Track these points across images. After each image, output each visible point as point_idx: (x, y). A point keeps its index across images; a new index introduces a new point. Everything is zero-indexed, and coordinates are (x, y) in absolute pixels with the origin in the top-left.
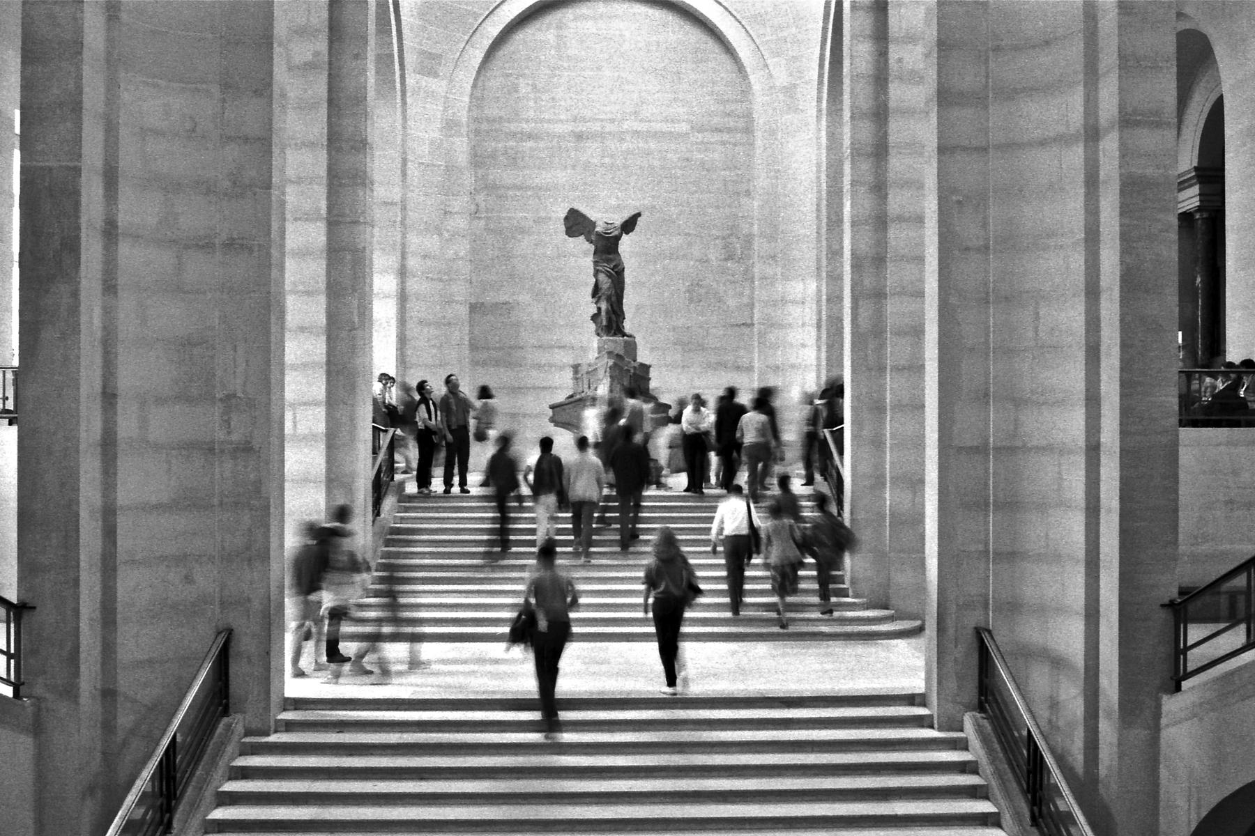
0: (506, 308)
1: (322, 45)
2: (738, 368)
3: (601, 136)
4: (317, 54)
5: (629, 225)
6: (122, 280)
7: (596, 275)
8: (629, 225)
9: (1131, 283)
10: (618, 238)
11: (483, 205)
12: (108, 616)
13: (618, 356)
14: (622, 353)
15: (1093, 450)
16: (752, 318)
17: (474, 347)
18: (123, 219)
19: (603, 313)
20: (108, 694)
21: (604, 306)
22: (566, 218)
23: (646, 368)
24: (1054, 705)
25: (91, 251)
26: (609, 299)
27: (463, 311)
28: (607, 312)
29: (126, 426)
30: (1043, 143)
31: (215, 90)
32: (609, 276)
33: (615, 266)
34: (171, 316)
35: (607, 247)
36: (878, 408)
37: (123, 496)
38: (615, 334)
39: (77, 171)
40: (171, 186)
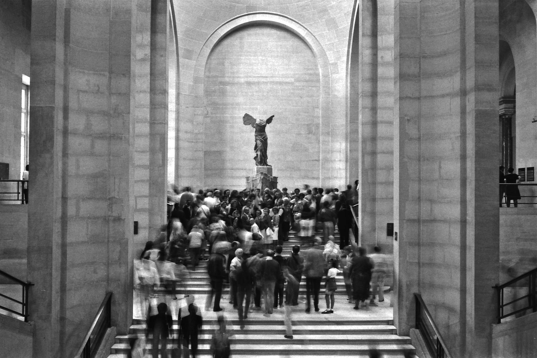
1: (148, 51)
3: (258, 83)
4: (146, 55)
5: (269, 121)
6: (70, 152)
8: (269, 121)
9: (479, 155)
10: (265, 126)
12: (63, 289)
14: (266, 173)
15: (463, 222)
16: (319, 157)
17: (206, 169)
18: (70, 127)
19: (259, 156)
20: (62, 319)
22: (244, 117)
23: (276, 178)
24: (448, 327)
25: (58, 139)
26: (261, 151)
27: (201, 154)
28: (260, 156)
29: (71, 211)
30: (443, 96)
31: (107, 74)
32: (261, 141)
33: (264, 137)
34: (88, 166)
35: (261, 130)
36: (374, 200)
37: (70, 239)
38: (264, 165)
39: (53, 108)
40: (89, 113)
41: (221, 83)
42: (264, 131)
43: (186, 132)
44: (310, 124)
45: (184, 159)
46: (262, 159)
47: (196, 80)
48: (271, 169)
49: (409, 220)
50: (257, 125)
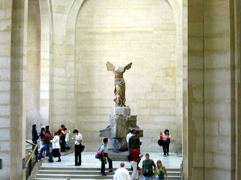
0: (89, 93)
1: (9, 23)
2: (170, 115)
3: (122, 32)
5: (128, 67)
7: (115, 86)
8: (128, 67)
10: (122, 73)
11: (80, 58)
13: (120, 115)
16: (175, 97)
17: (78, 108)
21: (118, 96)
22: (107, 64)
23: (135, 117)
27: (72, 95)
32: (120, 86)
33: (122, 83)
35: (120, 76)
41: (91, 33)
42: (122, 77)
43: (60, 76)
44: (167, 68)
45: (58, 99)
46: (121, 101)
47: (69, 32)
48: (129, 110)
49: (196, 168)
50: (116, 72)
